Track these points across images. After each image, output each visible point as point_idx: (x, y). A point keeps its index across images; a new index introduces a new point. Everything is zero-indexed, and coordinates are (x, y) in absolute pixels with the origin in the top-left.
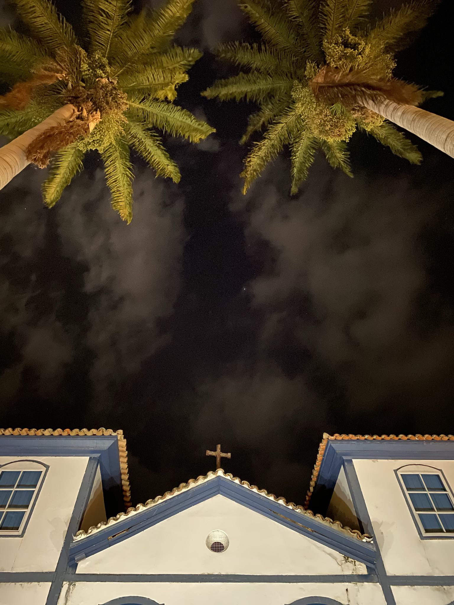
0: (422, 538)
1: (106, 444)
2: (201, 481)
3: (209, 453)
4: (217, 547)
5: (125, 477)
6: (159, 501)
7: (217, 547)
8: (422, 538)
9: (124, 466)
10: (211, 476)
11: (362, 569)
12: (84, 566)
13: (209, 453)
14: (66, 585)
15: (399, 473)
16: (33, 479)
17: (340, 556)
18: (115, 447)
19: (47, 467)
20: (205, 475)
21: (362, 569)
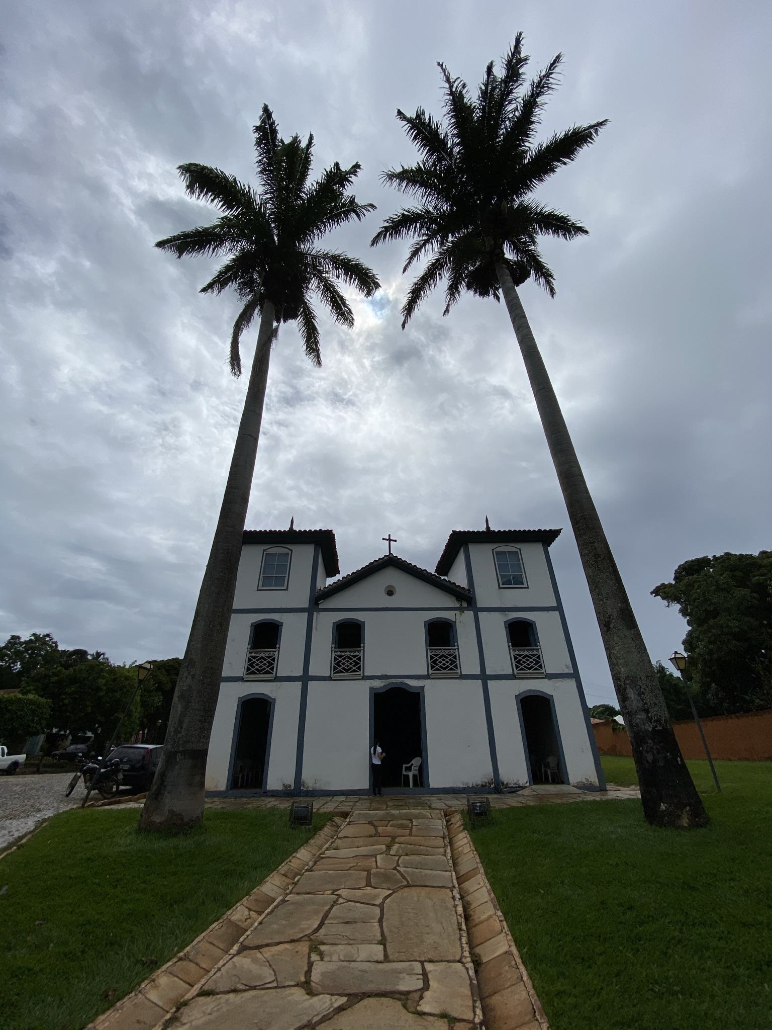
7: (390, 593)
8: (500, 588)
14: (315, 614)
17: (454, 598)
21: (465, 605)
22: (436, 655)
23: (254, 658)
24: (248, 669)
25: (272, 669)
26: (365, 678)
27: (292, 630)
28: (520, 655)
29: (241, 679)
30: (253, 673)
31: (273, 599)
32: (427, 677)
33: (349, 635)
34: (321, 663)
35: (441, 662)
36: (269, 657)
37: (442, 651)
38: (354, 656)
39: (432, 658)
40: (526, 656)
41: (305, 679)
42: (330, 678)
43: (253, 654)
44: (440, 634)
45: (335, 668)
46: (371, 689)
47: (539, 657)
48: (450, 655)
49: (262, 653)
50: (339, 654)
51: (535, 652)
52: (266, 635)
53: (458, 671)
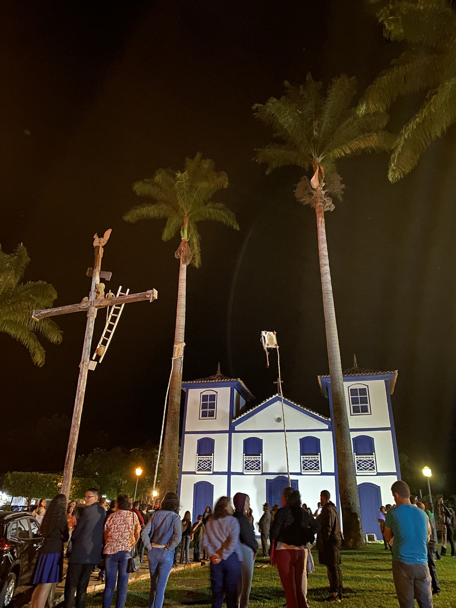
0: (351, 415)
1: (236, 383)
2: (270, 399)
3: (274, 383)
4: (279, 420)
5: (246, 388)
6: (257, 407)
7: (279, 420)
8: (351, 415)
9: (243, 385)
10: (274, 396)
11: (327, 427)
12: (237, 428)
13: (274, 383)
15: (349, 388)
16: (213, 398)
18: (239, 384)
19: (217, 392)
20: (272, 397)
21: (327, 427)
22: (306, 461)
23: (201, 461)
24: (198, 468)
25: (211, 467)
26: (263, 474)
27: (221, 442)
28: (360, 461)
29: (194, 473)
30: (200, 470)
31: (208, 424)
32: (300, 474)
33: (253, 447)
34: (238, 466)
35: (309, 465)
36: (209, 461)
37: (310, 458)
38: (257, 461)
39: (303, 462)
40: (365, 461)
41: (229, 473)
42: (242, 474)
43: (200, 459)
44: (310, 446)
45: (246, 468)
46: (267, 480)
47: (373, 462)
48: (315, 460)
49: (205, 458)
50: (247, 459)
51: (371, 459)
52: (206, 447)
53: (320, 471)
